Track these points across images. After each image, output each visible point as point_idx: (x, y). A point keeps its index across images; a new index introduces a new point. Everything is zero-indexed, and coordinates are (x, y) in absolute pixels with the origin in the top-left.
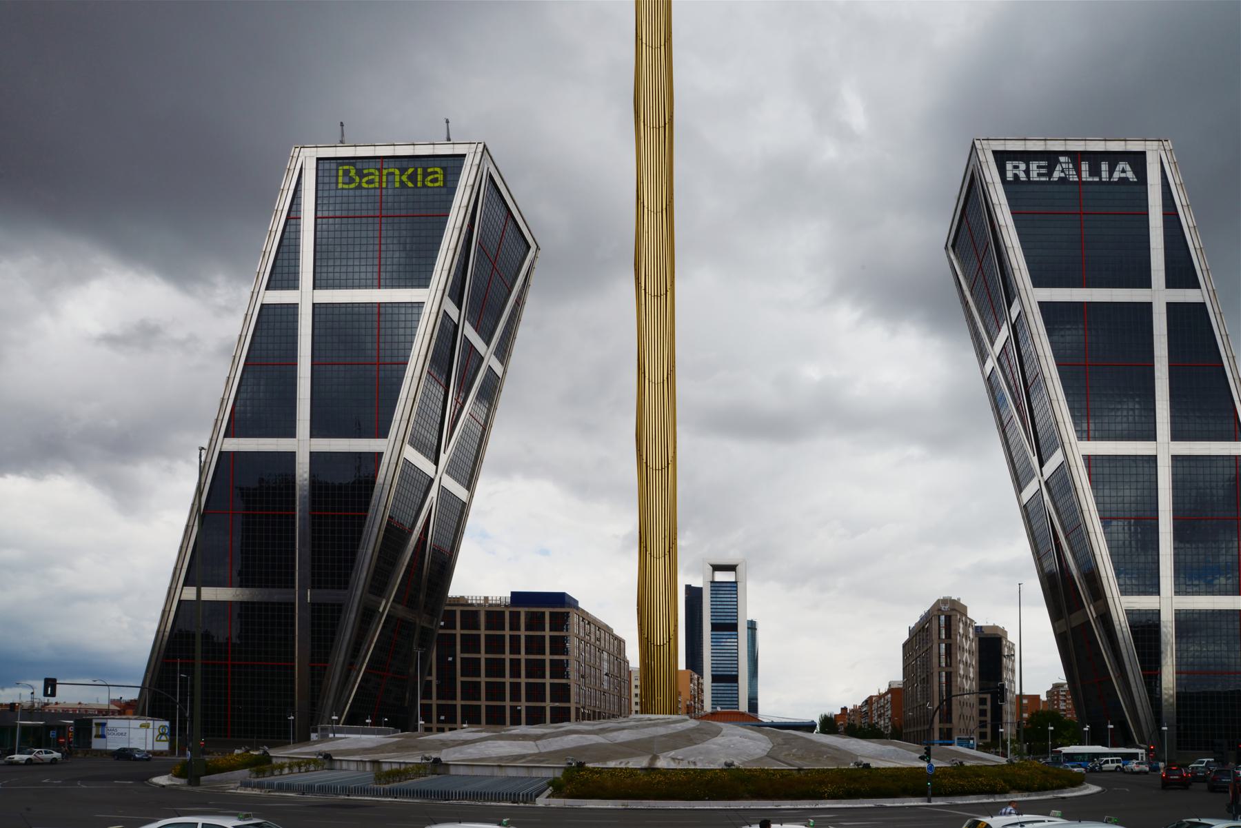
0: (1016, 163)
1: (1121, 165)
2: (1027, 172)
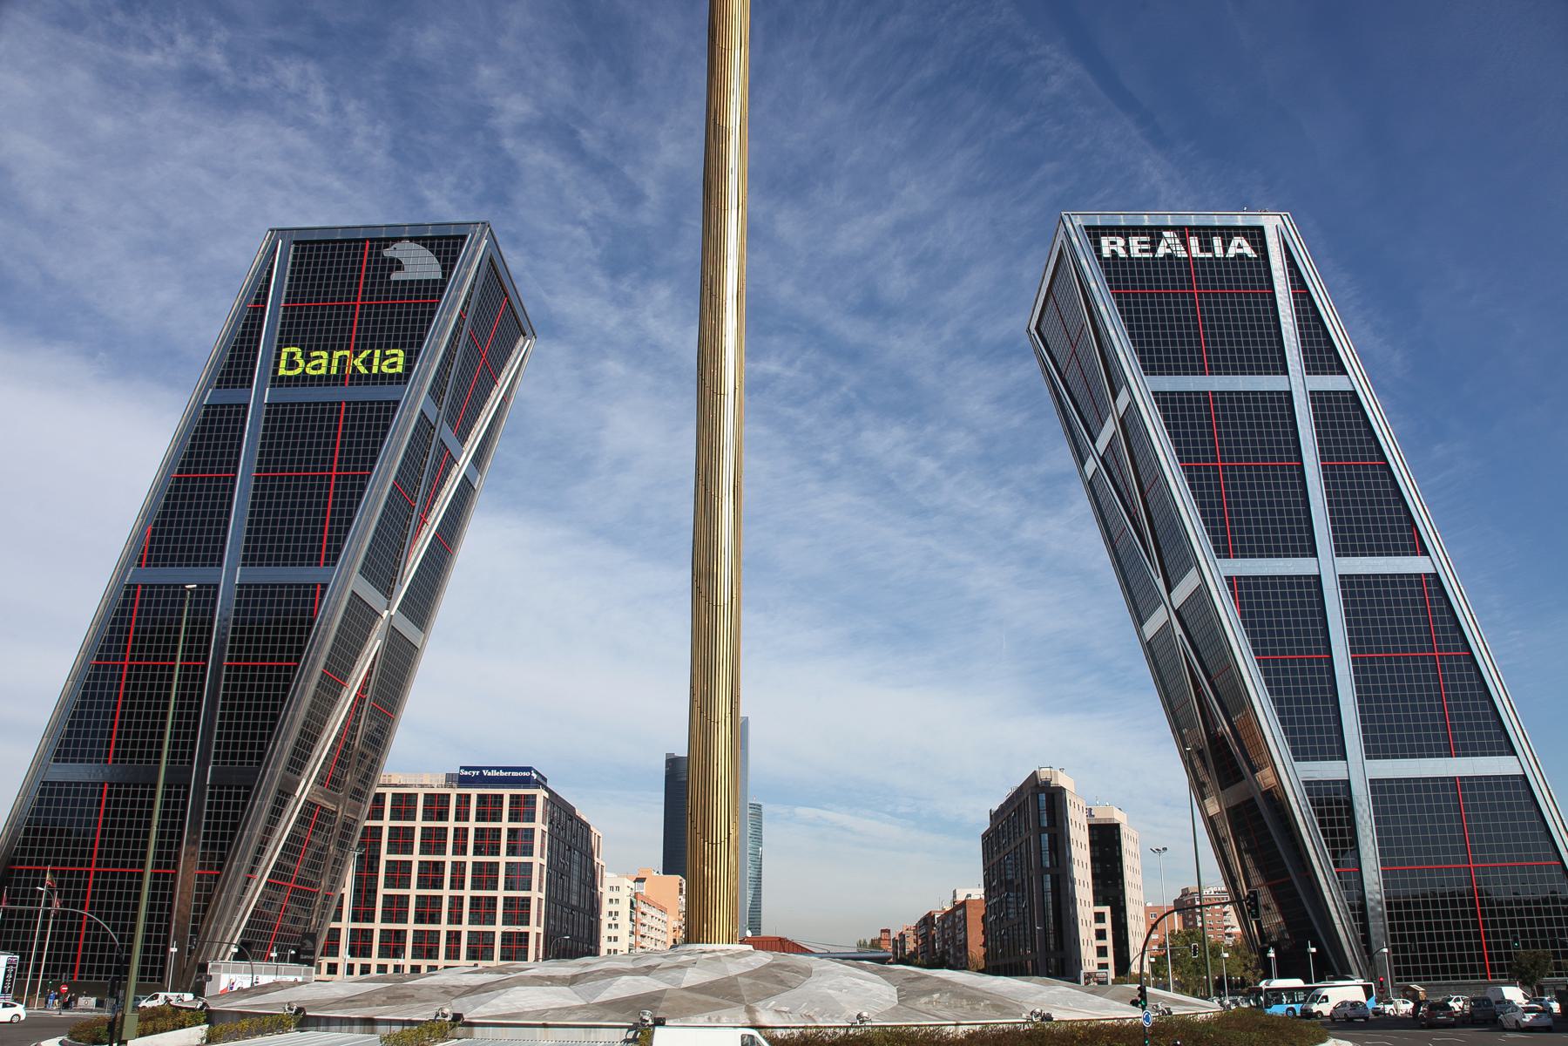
0: (1112, 239)
1: (1236, 240)
2: (1127, 248)
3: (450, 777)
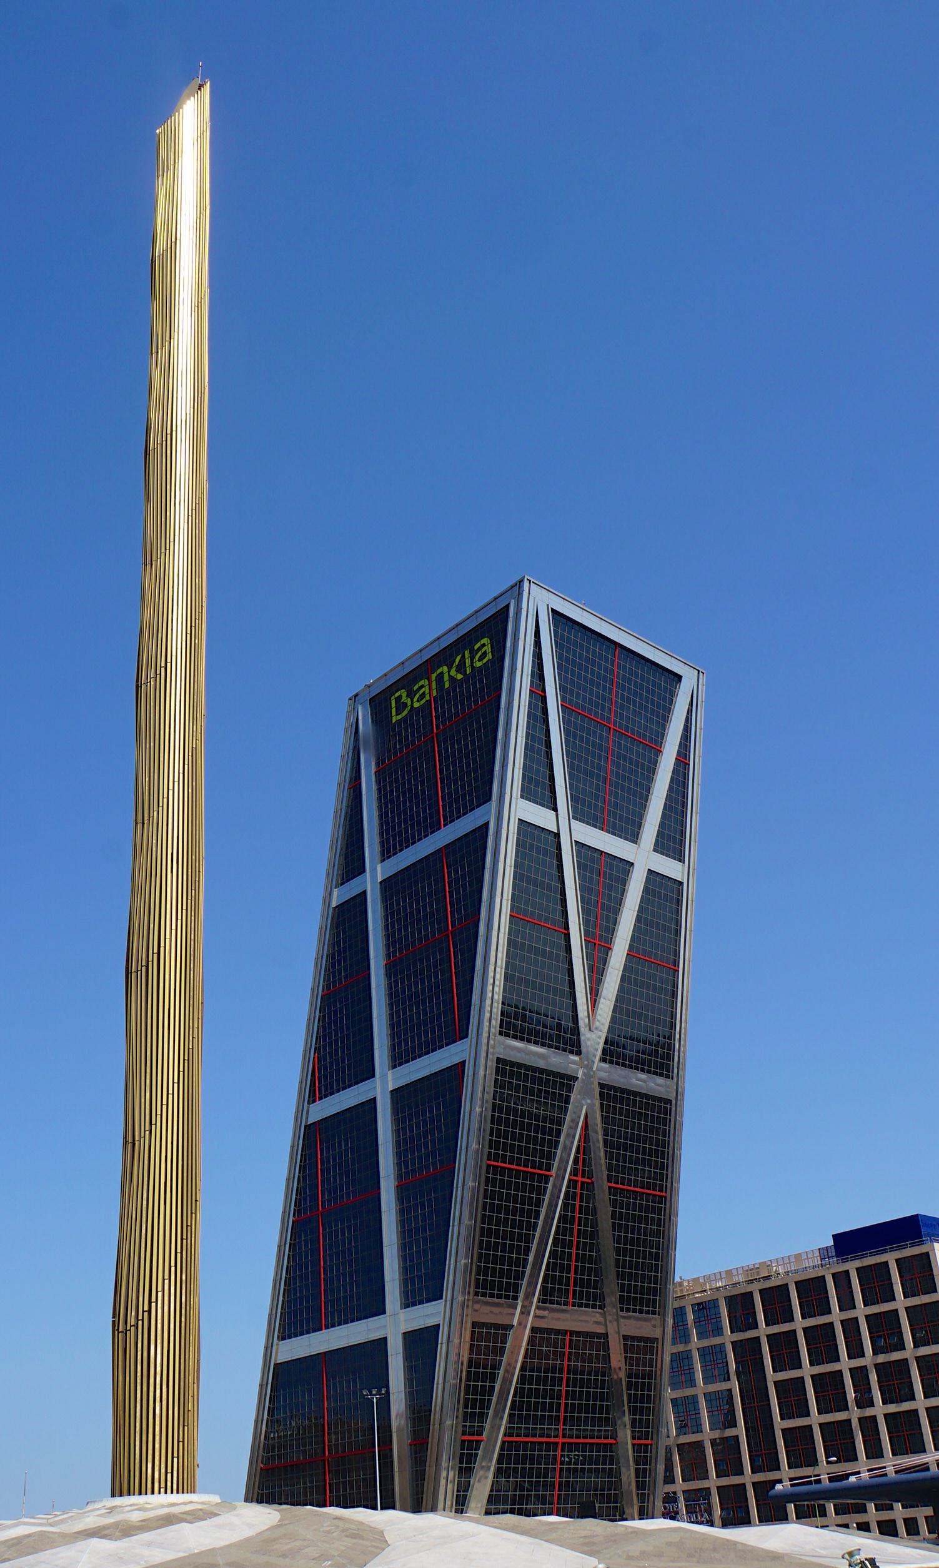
3: (824, 1252)
